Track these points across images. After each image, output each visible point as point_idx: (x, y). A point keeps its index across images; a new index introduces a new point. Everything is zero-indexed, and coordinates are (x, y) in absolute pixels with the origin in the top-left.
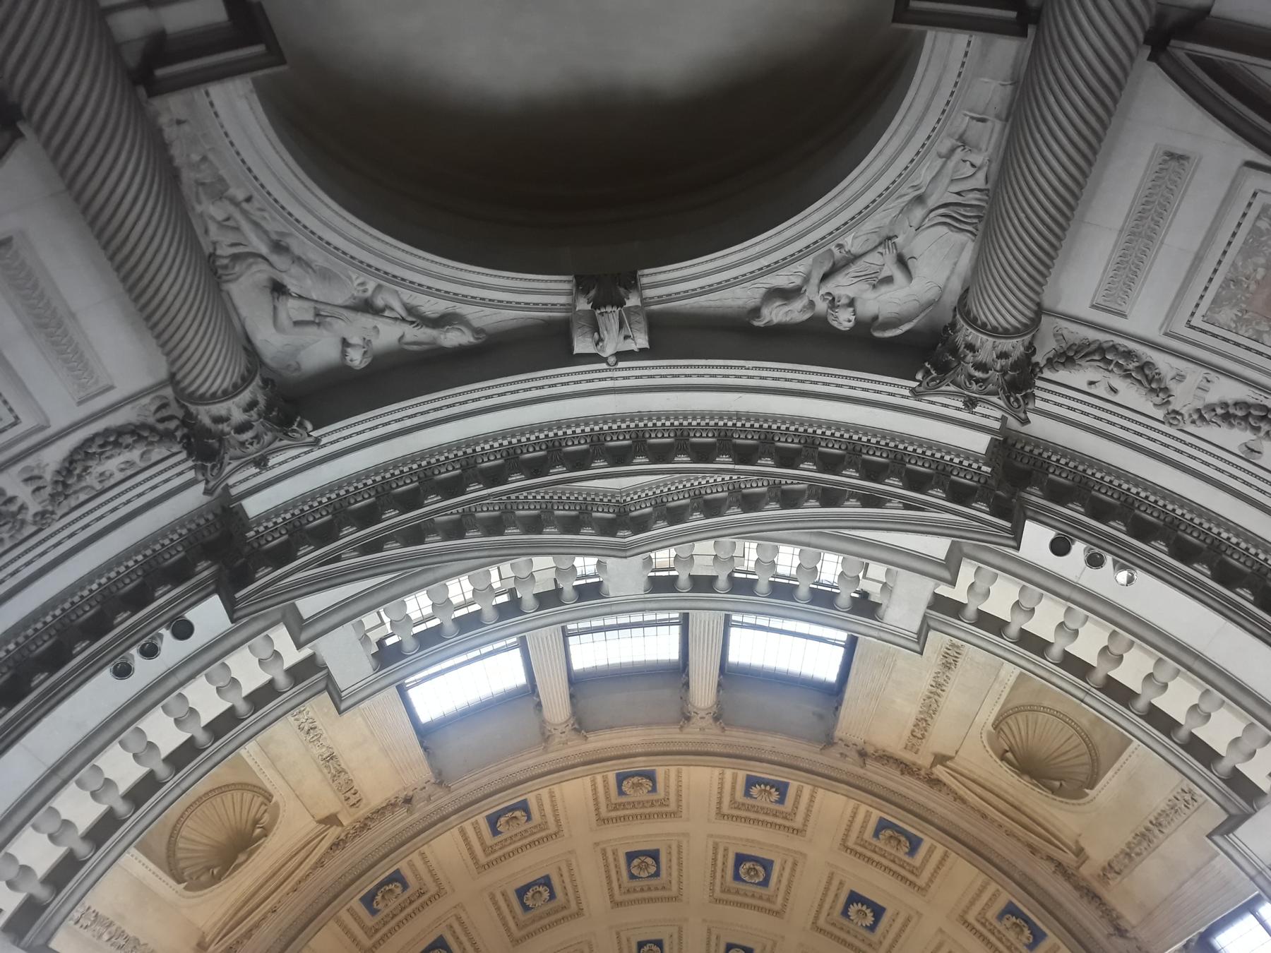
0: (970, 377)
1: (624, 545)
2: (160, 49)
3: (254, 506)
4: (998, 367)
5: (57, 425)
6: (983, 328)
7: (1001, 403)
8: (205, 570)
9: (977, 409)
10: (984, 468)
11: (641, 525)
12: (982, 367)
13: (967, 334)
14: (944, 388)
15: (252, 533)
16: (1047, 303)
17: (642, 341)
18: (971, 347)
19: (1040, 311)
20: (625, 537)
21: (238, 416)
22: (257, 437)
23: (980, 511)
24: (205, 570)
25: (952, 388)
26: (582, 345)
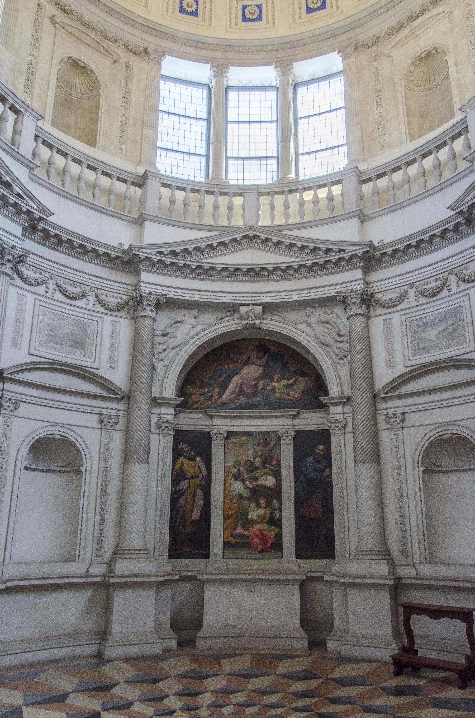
0: (151, 301)
1: (251, 230)
2: (344, 404)
3: (358, 274)
4: (144, 306)
5: (399, 313)
6: (151, 318)
7: (142, 294)
8: (378, 254)
9: (148, 292)
10: (141, 267)
11: (245, 237)
12: (149, 305)
13: (153, 315)
14: (158, 297)
15: (361, 264)
16: (133, 321)
17: (243, 309)
18: (152, 311)
19: (134, 319)
20: (251, 233)
21: (354, 307)
22: (352, 299)
23: (142, 256)
24: (378, 254)
25: (155, 297)
26: (259, 309)
